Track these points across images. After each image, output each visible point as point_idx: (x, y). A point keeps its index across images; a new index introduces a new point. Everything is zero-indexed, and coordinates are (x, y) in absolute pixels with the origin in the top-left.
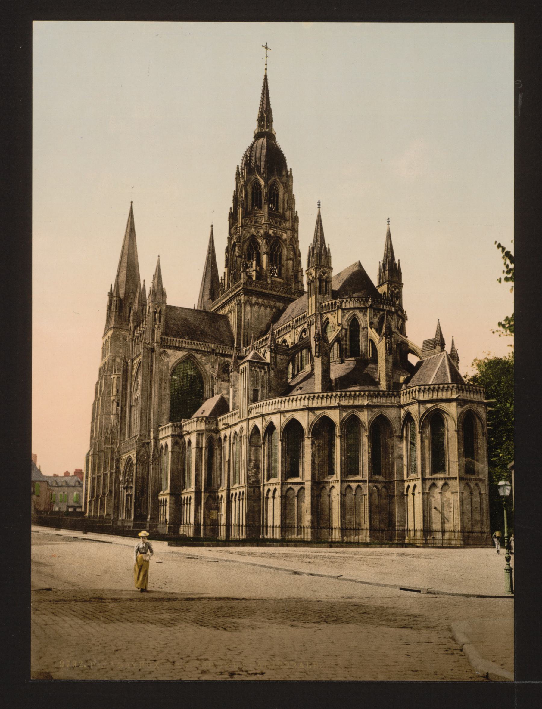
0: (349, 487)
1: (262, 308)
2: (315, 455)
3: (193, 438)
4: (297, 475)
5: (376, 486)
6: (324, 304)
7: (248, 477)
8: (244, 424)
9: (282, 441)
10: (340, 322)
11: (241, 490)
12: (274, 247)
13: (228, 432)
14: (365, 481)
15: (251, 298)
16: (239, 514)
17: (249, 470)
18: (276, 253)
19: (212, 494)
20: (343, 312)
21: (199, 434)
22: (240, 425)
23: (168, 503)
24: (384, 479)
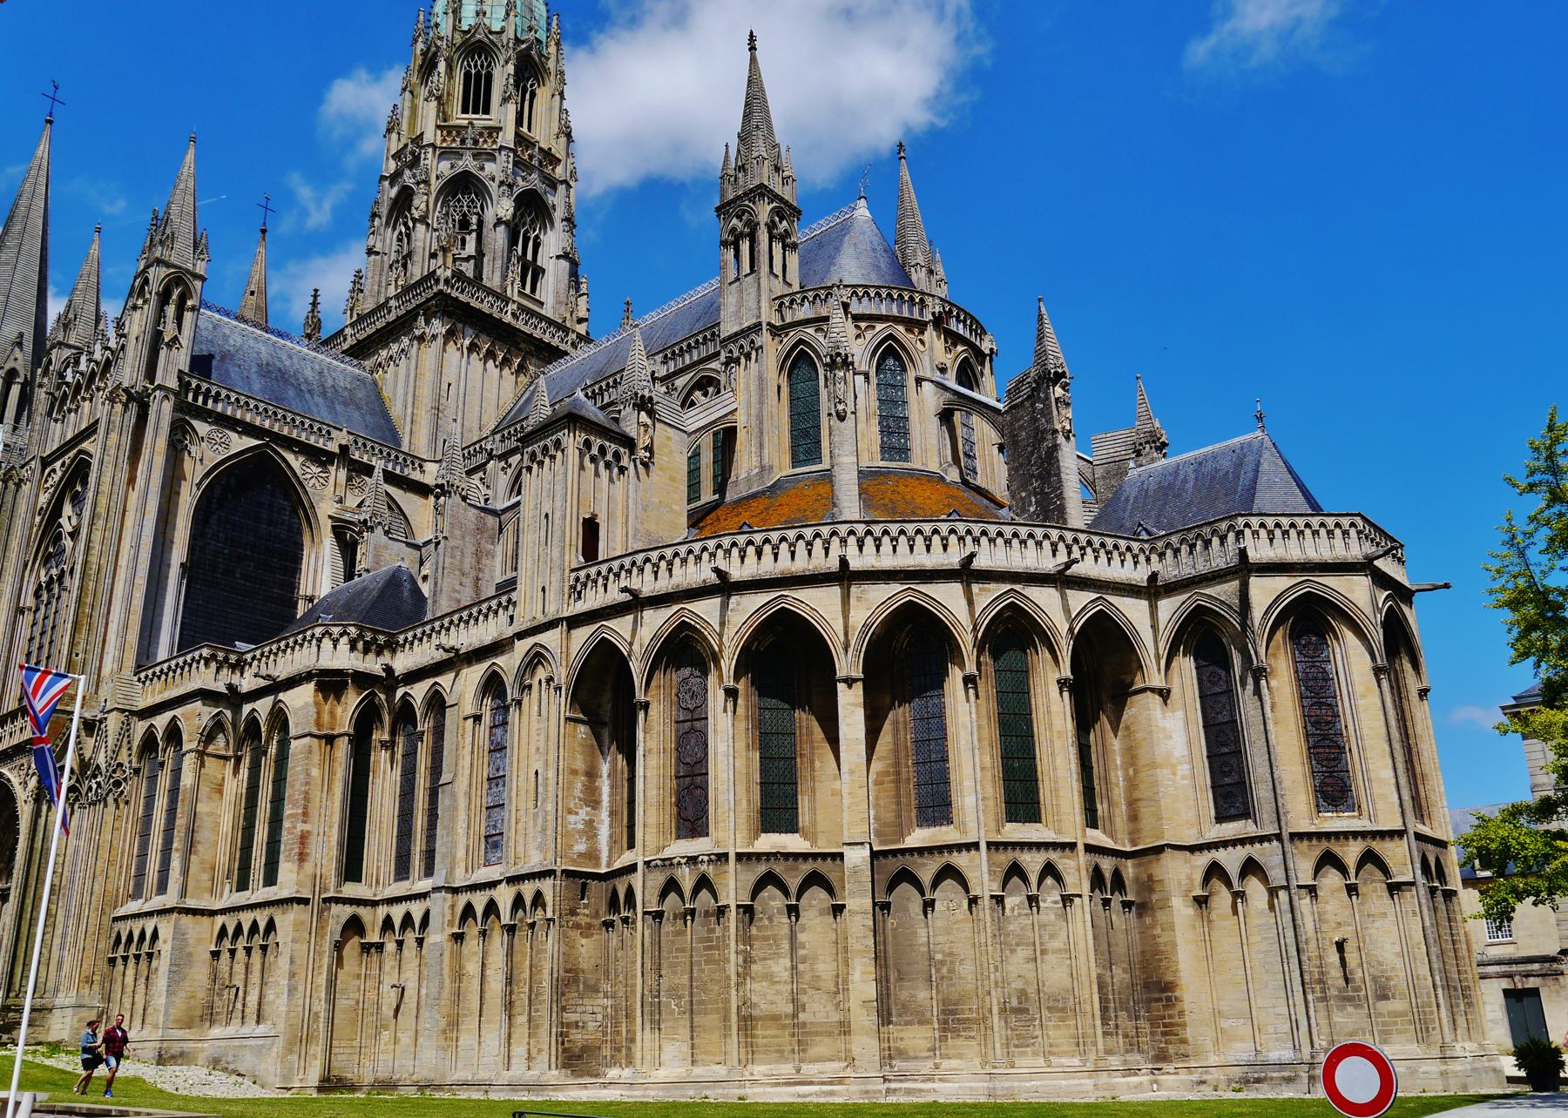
1: (490, 363)
3: (300, 700)
4: (792, 827)
6: (787, 301)
7: (562, 836)
8: (550, 639)
9: (731, 693)
11: (528, 890)
12: (522, 216)
13: (445, 680)
16: (510, 981)
17: (570, 812)
18: (527, 232)
19: (363, 912)
20: (857, 327)
22: (522, 647)
23: (165, 946)
24: (1108, 843)
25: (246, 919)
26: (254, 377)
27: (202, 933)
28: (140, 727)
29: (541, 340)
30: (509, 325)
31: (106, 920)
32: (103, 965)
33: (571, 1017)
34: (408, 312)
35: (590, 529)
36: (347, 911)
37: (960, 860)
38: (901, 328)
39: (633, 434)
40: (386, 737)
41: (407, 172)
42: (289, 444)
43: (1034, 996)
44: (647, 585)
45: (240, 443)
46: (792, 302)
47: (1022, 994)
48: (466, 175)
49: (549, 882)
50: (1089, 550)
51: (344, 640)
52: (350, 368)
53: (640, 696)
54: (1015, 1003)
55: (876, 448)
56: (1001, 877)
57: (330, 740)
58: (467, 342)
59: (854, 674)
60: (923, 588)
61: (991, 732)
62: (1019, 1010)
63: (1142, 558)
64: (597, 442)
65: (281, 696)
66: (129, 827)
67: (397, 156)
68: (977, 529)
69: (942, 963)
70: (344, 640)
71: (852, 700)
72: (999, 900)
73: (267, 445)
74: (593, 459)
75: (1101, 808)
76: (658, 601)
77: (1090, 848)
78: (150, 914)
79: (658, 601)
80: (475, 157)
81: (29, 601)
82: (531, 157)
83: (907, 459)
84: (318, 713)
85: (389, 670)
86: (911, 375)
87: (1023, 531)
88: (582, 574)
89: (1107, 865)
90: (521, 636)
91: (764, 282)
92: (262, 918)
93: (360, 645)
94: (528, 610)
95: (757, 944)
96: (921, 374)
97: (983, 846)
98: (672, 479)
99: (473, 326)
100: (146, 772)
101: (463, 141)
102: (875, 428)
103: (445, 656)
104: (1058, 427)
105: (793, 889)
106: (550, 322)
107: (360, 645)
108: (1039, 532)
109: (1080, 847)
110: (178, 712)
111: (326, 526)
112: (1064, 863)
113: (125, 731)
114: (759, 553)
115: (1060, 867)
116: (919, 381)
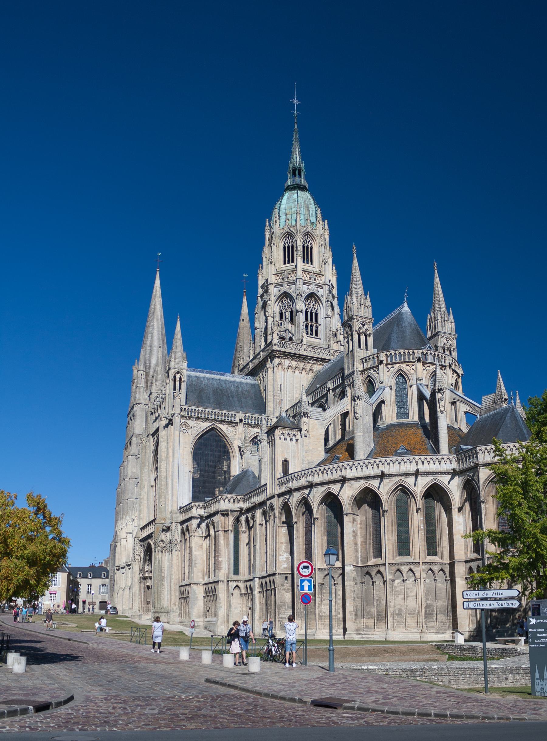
0: (399, 570)
2: (356, 534)
5: (431, 569)
6: (364, 360)
10: (381, 379)
11: (271, 578)
14: (419, 563)
15: (283, 360)
17: (281, 555)
18: (311, 310)
21: (223, 515)
22: (268, 503)
25: (210, 586)
26: (211, 396)
27: (199, 592)
28: (179, 528)
29: (318, 358)
30: (303, 355)
31: (178, 587)
32: (178, 600)
33: (281, 616)
34: (265, 358)
35: (286, 463)
36: (235, 584)
37: (382, 569)
38: (404, 365)
39: (302, 427)
40: (244, 529)
41: (265, 295)
42: (221, 422)
43: (404, 610)
44: (294, 484)
45: (205, 425)
46: (366, 360)
47: (400, 610)
48: (285, 293)
49: (276, 576)
50: (431, 461)
51: (227, 500)
52: (249, 380)
53: (294, 520)
54: (397, 612)
55: (395, 415)
56: (393, 574)
57: (225, 531)
58: (286, 366)
59: (348, 512)
60: (371, 482)
61: (395, 528)
62: (399, 614)
63: (454, 460)
64: (286, 432)
65: (213, 518)
66: (180, 559)
67: (262, 287)
68: (388, 459)
69: (377, 600)
70: (227, 500)
71: (348, 520)
72: (393, 581)
73: (213, 424)
74: (285, 439)
75: (439, 549)
76: (297, 489)
77: (425, 563)
78: (186, 585)
79: (297, 489)
80: (288, 284)
81: (153, 483)
82: (310, 278)
83: (408, 417)
84: (222, 524)
85: (241, 509)
86: (408, 384)
87: (405, 458)
88: (280, 480)
89: (436, 568)
90: (269, 499)
91: (356, 354)
92: (212, 586)
93: (232, 500)
94: (270, 491)
95: (325, 595)
96: (412, 383)
97: (387, 565)
98: (317, 439)
99: (288, 358)
100: (183, 541)
101: (283, 279)
102: (394, 407)
103: (253, 505)
104: (438, 410)
105: (335, 579)
106: (322, 348)
107: (232, 500)
108: (411, 458)
109: (421, 564)
110: (188, 523)
111: (237, 449)
112: (416, 569)
113: (176, 529)
114: (323, 473)
115: (414, 570)
116: (411, 386)
